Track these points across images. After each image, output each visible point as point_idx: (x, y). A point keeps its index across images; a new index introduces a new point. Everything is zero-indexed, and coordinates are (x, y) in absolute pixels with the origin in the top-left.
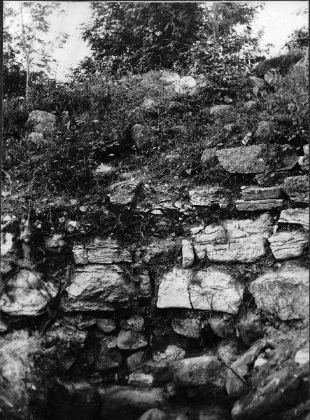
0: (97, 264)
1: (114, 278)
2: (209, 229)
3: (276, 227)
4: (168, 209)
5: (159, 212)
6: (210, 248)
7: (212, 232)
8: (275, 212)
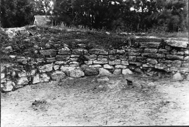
0: (23, 77)
1: (27, 79)
2: (42, 67)
3: (54, 65)
4: (34, 64)
5: (32, 65)
6: (42, 70)
7: (43, 67)
8: (54, 62)
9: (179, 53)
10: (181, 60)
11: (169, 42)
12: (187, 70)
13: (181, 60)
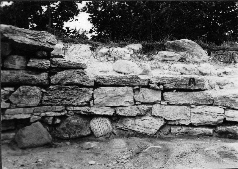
9: (34, 63)
10: (40, 85)
11: (6, 31)
12: (56, 112)
13: (40, 85)
